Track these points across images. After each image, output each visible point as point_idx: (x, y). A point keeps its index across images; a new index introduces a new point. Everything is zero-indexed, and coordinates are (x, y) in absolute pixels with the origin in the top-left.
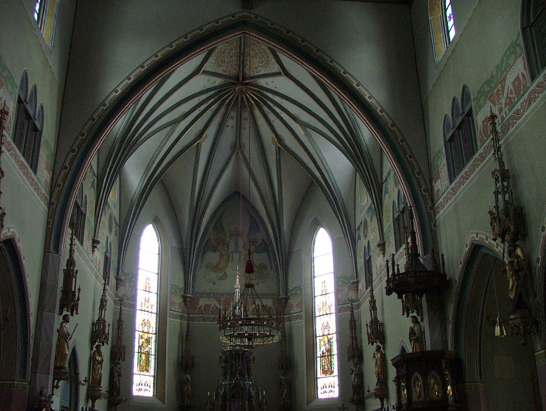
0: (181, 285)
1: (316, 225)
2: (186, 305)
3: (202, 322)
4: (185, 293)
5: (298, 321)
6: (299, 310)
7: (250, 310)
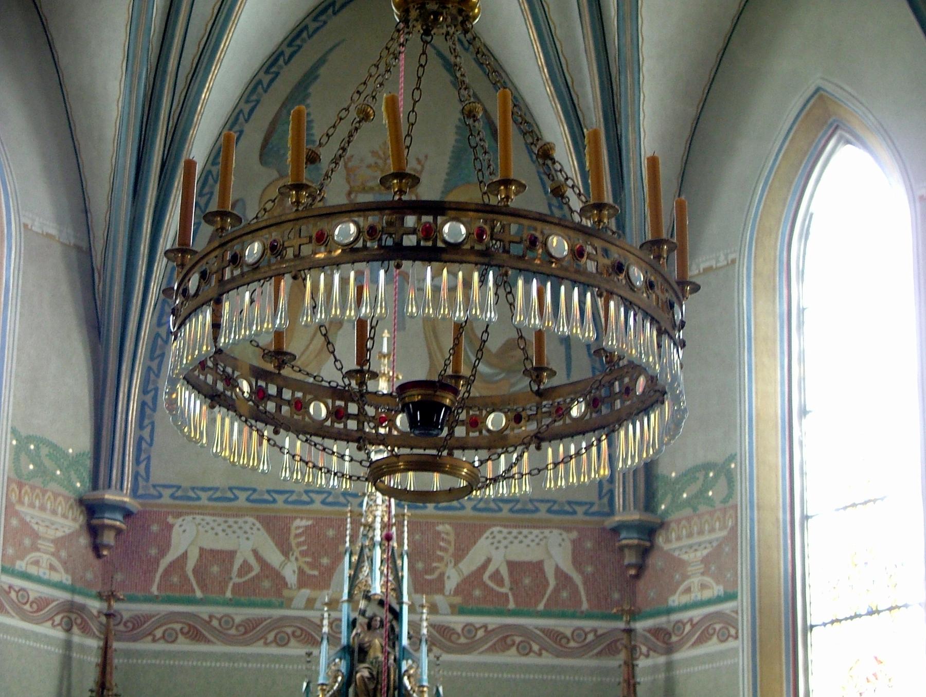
0: (77, 440)
1: (821, 122)
2: (97, 549)
3: (183, 645)
4: (95, 486)
5: (713, 646)
6: (718, 589)
7: (451, 584)
